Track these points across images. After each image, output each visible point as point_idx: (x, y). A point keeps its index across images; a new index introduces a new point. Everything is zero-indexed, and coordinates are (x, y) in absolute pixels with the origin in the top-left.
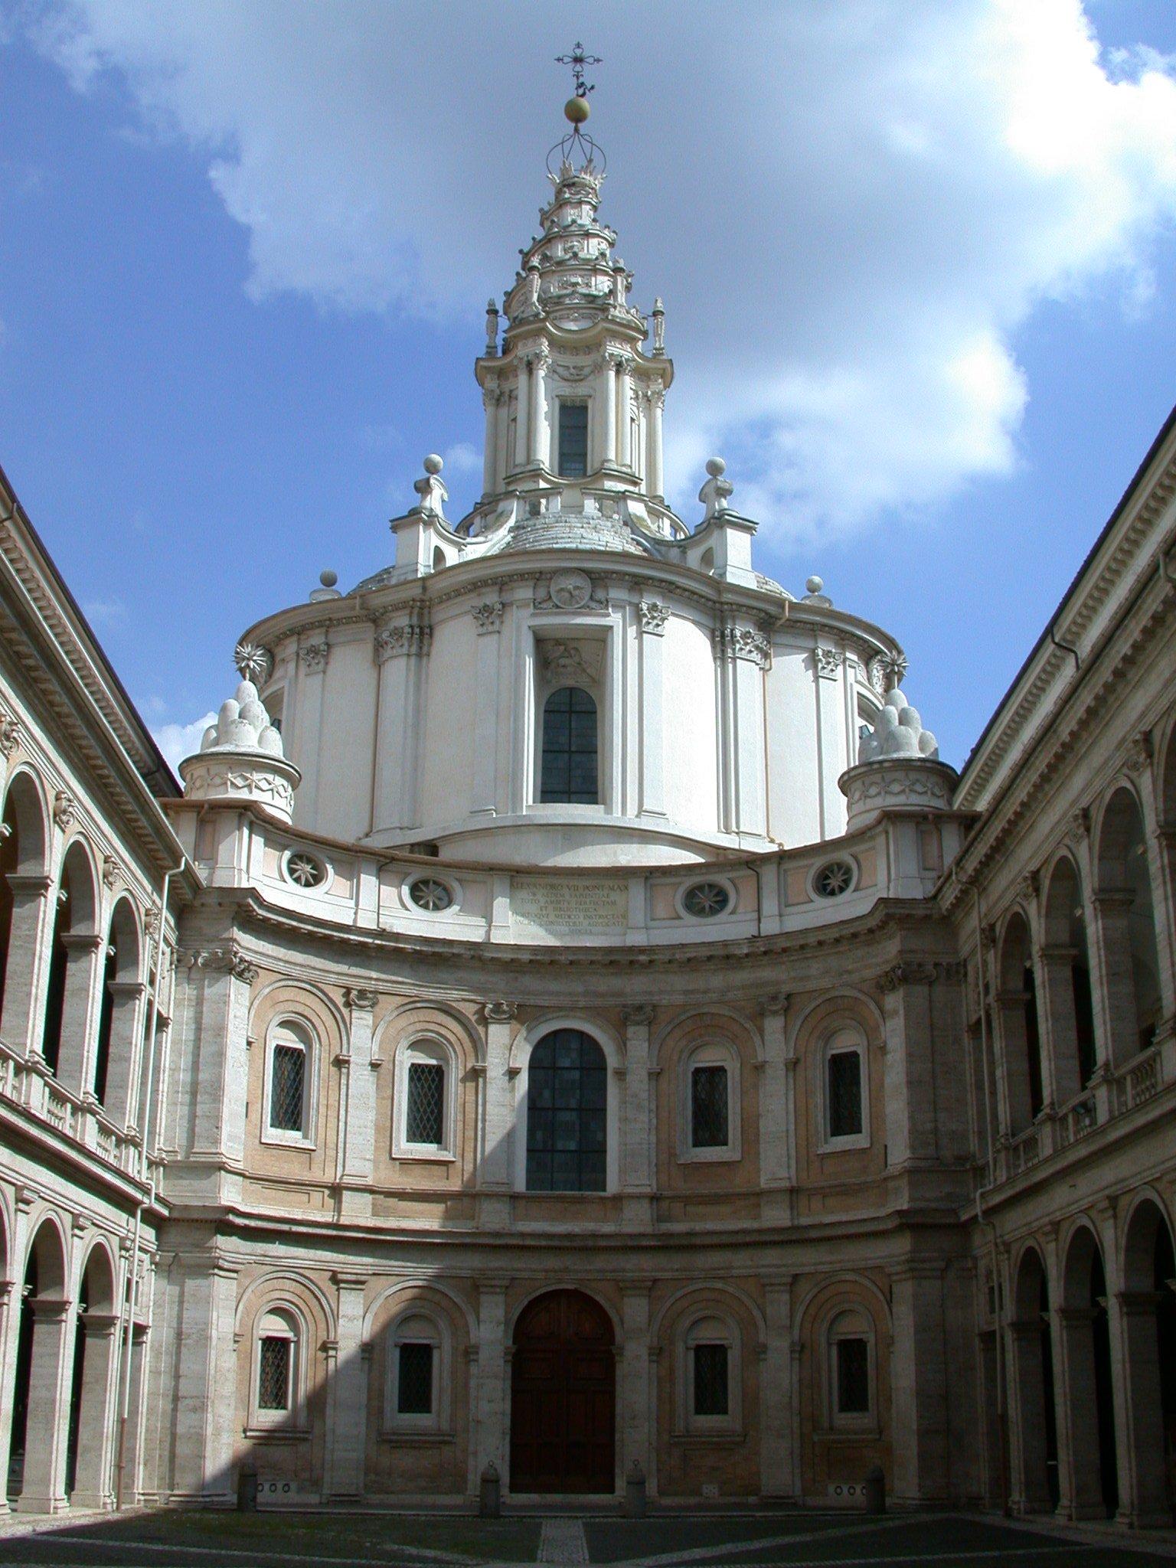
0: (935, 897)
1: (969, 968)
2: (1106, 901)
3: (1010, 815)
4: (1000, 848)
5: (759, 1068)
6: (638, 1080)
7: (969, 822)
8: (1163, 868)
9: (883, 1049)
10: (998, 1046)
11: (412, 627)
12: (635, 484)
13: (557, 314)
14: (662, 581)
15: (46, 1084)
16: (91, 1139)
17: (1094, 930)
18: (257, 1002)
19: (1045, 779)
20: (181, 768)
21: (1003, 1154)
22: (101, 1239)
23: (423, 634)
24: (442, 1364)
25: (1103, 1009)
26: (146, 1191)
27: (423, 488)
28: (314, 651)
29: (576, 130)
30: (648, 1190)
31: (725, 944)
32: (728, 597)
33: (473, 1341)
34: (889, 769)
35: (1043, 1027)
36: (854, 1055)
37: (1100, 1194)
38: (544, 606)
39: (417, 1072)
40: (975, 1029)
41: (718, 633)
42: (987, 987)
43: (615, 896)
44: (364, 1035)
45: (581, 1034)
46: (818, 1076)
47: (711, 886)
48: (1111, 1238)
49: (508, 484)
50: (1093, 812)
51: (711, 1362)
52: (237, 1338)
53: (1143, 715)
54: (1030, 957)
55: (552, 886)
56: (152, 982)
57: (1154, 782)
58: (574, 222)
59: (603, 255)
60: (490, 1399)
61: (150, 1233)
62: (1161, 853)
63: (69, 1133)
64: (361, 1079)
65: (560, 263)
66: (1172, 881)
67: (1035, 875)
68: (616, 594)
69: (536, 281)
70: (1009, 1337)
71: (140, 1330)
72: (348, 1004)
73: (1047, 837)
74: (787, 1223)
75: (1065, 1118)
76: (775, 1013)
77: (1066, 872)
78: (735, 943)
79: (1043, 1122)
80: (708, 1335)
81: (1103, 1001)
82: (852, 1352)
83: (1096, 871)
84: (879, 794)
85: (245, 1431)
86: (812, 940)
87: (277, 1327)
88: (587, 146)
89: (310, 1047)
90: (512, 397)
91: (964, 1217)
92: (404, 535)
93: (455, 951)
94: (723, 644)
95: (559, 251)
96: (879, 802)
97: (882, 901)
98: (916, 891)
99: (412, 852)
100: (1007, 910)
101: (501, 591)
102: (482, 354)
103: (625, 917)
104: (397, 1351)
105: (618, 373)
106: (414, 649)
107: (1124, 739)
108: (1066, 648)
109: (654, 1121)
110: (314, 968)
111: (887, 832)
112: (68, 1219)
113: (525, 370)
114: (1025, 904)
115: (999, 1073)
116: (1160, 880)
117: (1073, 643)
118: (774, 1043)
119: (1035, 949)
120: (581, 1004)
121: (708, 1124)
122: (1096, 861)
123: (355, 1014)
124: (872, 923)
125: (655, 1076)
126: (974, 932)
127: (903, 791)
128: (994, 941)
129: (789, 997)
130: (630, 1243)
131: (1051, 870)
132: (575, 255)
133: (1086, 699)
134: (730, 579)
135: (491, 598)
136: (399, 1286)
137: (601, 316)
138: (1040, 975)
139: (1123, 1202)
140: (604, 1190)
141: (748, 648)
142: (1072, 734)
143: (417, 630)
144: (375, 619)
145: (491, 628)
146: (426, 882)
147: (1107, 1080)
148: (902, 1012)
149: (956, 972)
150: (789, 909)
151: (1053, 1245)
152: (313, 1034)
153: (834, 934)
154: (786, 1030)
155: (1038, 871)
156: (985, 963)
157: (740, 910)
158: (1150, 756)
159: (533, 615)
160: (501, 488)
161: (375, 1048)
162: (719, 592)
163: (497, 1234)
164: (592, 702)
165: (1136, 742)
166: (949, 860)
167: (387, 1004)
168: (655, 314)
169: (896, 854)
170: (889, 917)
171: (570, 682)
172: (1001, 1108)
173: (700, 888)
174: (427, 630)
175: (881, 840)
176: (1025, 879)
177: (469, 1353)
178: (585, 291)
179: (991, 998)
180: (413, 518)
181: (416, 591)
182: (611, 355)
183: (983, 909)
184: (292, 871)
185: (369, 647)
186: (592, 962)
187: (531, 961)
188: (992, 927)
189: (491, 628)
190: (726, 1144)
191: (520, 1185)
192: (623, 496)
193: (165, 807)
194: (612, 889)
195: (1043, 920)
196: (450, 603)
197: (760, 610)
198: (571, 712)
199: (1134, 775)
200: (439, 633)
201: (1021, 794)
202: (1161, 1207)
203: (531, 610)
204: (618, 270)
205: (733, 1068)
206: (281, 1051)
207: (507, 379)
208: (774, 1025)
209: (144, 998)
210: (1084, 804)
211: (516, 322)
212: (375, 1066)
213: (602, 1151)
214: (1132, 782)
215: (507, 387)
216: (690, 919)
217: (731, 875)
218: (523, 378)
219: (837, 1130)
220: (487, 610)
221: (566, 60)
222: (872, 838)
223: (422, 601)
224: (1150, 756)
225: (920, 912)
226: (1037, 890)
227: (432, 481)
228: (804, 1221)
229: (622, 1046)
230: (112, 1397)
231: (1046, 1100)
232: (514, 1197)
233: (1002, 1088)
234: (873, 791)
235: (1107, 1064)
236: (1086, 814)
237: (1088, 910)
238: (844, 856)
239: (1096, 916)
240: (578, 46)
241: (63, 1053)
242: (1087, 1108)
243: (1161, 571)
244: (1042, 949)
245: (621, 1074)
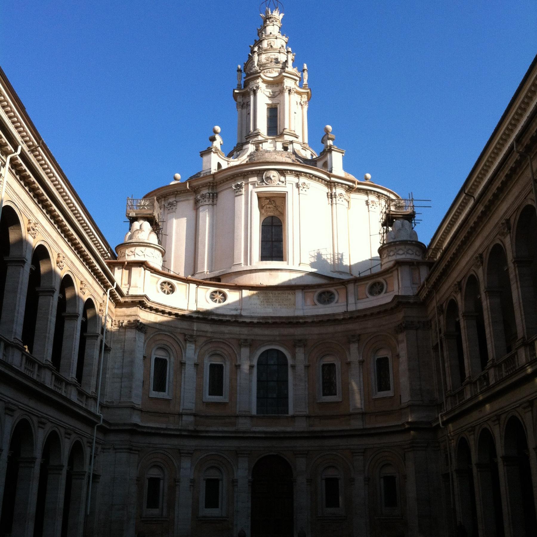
0: (417, 295)
1: (432, 322)
2: (490, 292)
3: (448, 259)
4: (445, 273)
5: (349, 364)
6: (300, 368)
7: (431, 265)
8: (516, 275)
9: (398, 356)
10: (445, 354)
11: (209, 194)
12: (297, 138)
13: (265, 71)
14: (307, 173)
15: (53, 374)
16: (74, 397)
17: (486, 303)
18: (147, 341)
19: (463, 243)
20: (116, 248)
21: (449, 399)
22: (79, 439)
23: (214, 197)
24: (224, 487)
25: (491, 336)
26: (99, 418)
27: (213, 139)
28: (171, 204)
30: (304, 413)
31: (334, 315)
32: (333, 179)
33: (235, 478)
34: (398, 245)
35: (465, 345)
36: (386, 359)
37: (493, 414)
39: (213, 367)
40: (435, 348)
41: (329, 194)
42: (440, 330)
43: (291, 297)
44: (191, 352)
45: (278, 351)
46: (372, 367)
47: (328, 292)
48: (497, 432)
49: (247, 139)
50: (484, 255)
51: (332, 485)
52: (138, 479)
53: (506, 212)
54: (458, 316)
55: (265, 294)
56: (102, 333)
57: (511, 240)
58: (271, 33)
59: (283, 46)
60: (243, 502)
61: (101, 436)
62: (515, 269)
63: (64, 394)
64: (190, 371)
65: (265, 50)
66: (520, 281)
67: (459, 283)
69: (256, 58)
70: (455, 476)
71: (96, 477)
72: (185, 340)
73: (464, 267)
74: (362, 427)
75: (475, 383)
76: (354, 342)
77: (473, 281)
78: (338, 314)
79: (466, 385)
80: (331, 473)
81: (490, 333)
82: (390, 481)
83: (486, 278)
84: (394, 254)
85: (141, 518)
86: (368, 313)
87: (154, 473)
89: (170, 358)
90: (248, 105)
91: (434, 425)
92: (205, 158)
93: (227, 319)
94: (332, 198)
96: (394, 258)
97: (396, 297)
98: (410, 292)
99: (210, 281)
100: (447, 299)
102: (236, 86)
103: (294, 305)
104: (205, 481)
105: (289, 94)
106: (211, 202)
107: (497, 223)
108: (470, 195)
109: (307, 385)
110: (171, 326)
111: (397, 270)
112: (62, 430)
114: (455, 295)
115: (446, 365)
116: (515, 281)
117: (473, 193)
118: (354, 354)
119: (460, 314)
120: (278, 338)
121: (329, 387)
122: (486, 275)
123: (188, 345)
124: (393, 305)
125: (307, 367)
126: (434, 307)
127: (404, 253)
128: (443, 311)
129: (359, 335)
130: (298, 435)
131: (466, 281)
132: (271, 46)
133: (481, 208)
136: (206, 455)
138: (462, 324)
139: (503, 417)
140: (288, 414)
142: (475, 223)
143: (211, 195)
144: (195, 190)
146: (216, 292)
147: (494, 366)
148: (405, 341)
149: (427, 325)
150: (359, 301)
151: (472, 437)
152: (171, 354)
153: (377, 310)
154: (358, 348)
155: (461, 281)
156: (439, 321)
157: (340, 301)
158: (509, 229)
160: (244, 141)
161: (196, 358)
162: (330, 178)
163: (244, 432)
164: (280, 222)
165: (502, 224)
166: (423, 280)
167: (201, 341)
168: (304, 70)
169: (402, 278)
170: (399, 303)
171: (272, 214)
172: (448, 379)
173: (323, 293)
174: (215, 195)
175: (395, 273)
176: (455, 285)
177: (234, 482)
179: (442, 335)
180: (209, 151)
181: (211, 179)
182: (286, 86)
183: (438, 299)
184: (162, 289)
185: (192, 202)
186: (282, 323)
187: (258, 323)
188: (442, 305)
190: (335, 394)
191: (254, 412)
192: (292, 142)
193: (109, 264)
194: (289, 294)
195: (463, 302)
196: (224, 184)
197: (346, 184)
199: (502, 238)
200: (221, 196)
201: (453, 250)
202: (520, 418)
203: (257, 186)
204: (288, 52)
205: (338, 364)
206: (157, 360)
207: (245, 98)
208: (354, 347)
209: (99, 338)
210: (480, 251)
211: (248, 75)
212: (196, 365)
213: (287, 397)
214: (502, 241)
215: (246, 101)
216: (320, 305)
217: (335, 288)
219: (380, 389)
222: (392, 272)
223: (213, 183)
224: (509, 229)
225: (411, 301)
226: (460, 289)
227: (217, 137)
228: (368, 426)
229: (294, 356)
230: (83, 507)
231: (467, 375)
232: (252, 417)
233: (448, 371)
234: (392, 254)
235: (493, 360)
236: (481, 256)
237: (483, 295)
238: (381, 279)
239: (486, 297)
241: (63, 362)
242: (486, 378)
243: (515, 148)
244: (463, 313)
245: (293, 367)
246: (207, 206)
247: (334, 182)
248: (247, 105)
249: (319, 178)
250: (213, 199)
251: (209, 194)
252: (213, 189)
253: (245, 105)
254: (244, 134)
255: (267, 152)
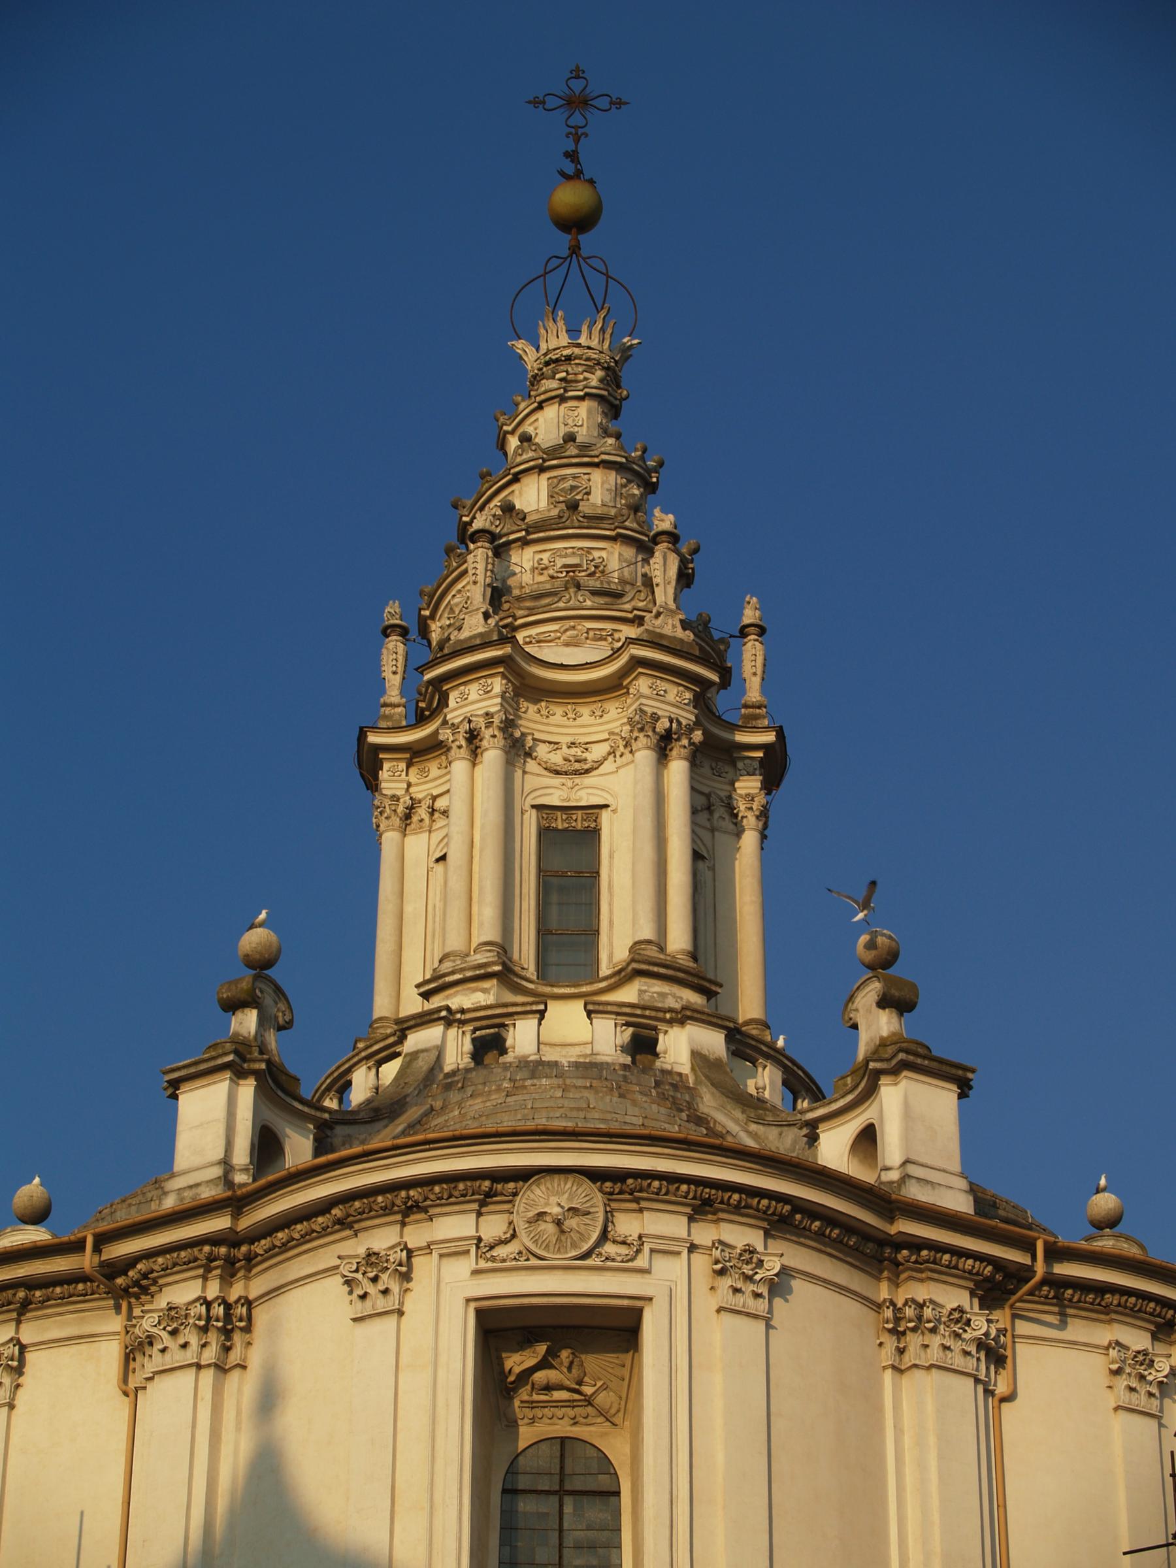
11: (208, 1304)
13: (533, 631)
29: (575, 250)
38: (501, 1251)
49: (426, 996)
58: (570, 438)
68: (667, 1224)
88: (597, 282)
95: (532, 496)
101: (403, 1224)
113: (464, 752)
132: (573, 506)
134: (916, 1193)
135: (382, 1238)
137: (631, 632)
141: (957, 1346)
143: (219, 1310)
145: (382, 1304)
159: (476, 1272)
160: (413, 1004)
178: (593, 583)
185: (111, 1352)
189: (382, 1304)
198: (561, 1493)
218: (460, 767)
220: (372, 1258)
221: (552, 102)
240: (577, 74)
246: (189, 1376)
247: (916, 1245)
248: (433, 811)
249: (830, 1218)
250: (227, 1333)
251: (208, 1304)
252: (228, 1278)
253: (422, 812)
254: (415, 971)
255: (536, 1068)
